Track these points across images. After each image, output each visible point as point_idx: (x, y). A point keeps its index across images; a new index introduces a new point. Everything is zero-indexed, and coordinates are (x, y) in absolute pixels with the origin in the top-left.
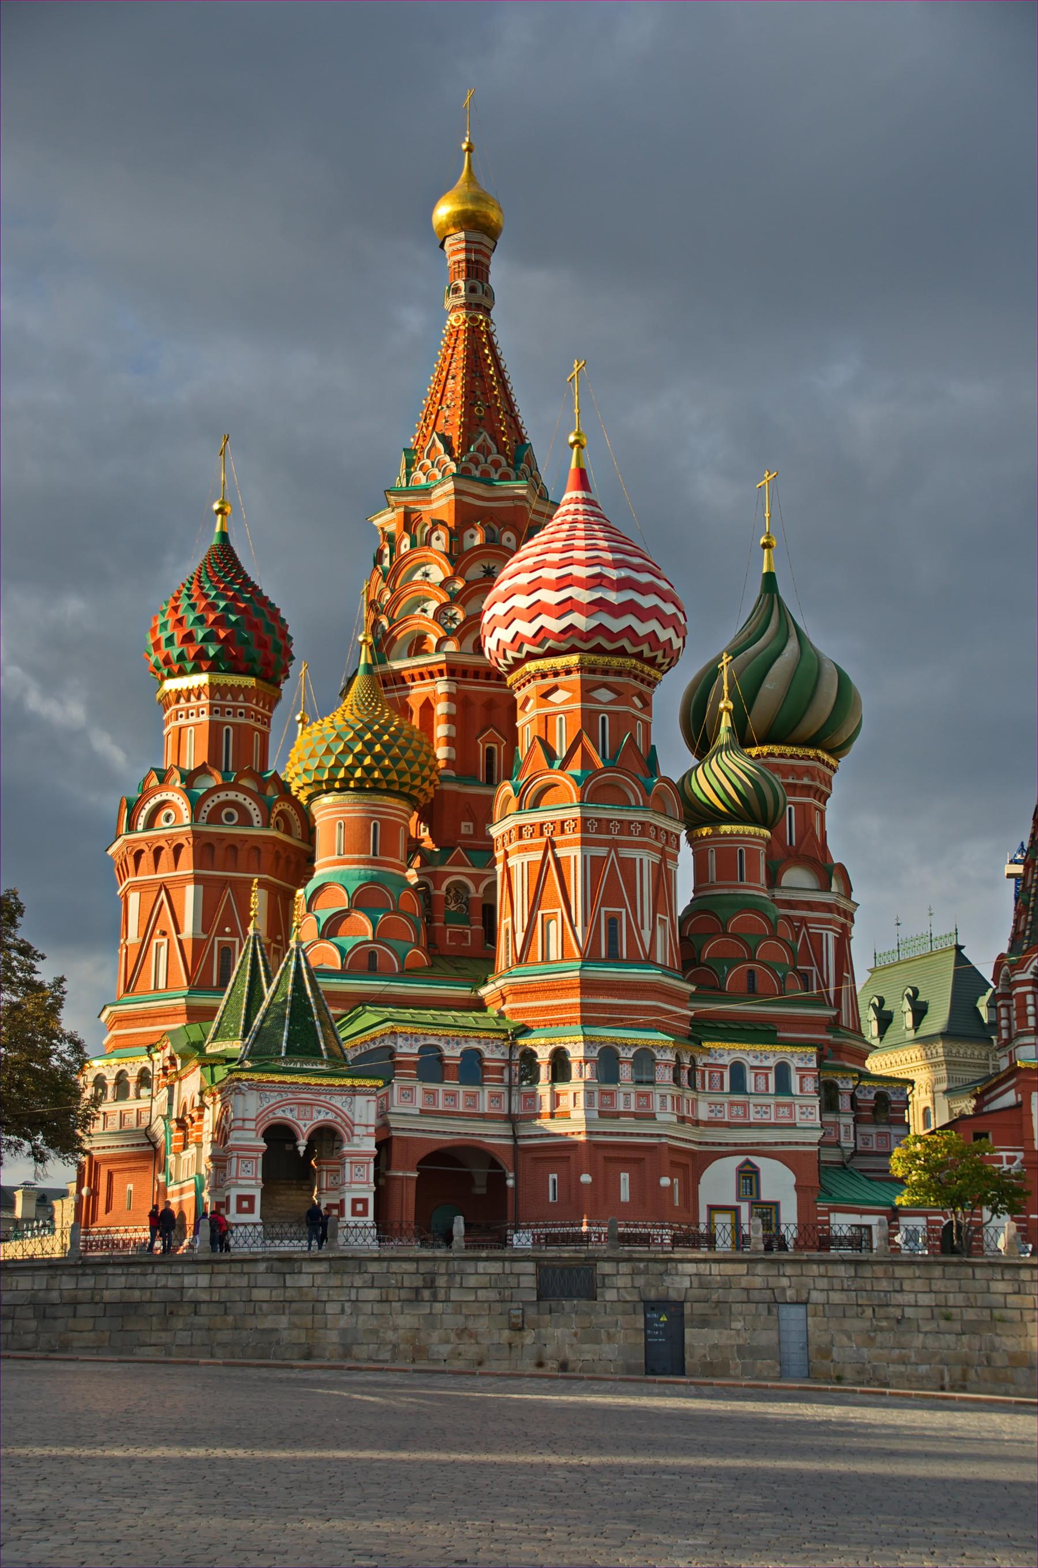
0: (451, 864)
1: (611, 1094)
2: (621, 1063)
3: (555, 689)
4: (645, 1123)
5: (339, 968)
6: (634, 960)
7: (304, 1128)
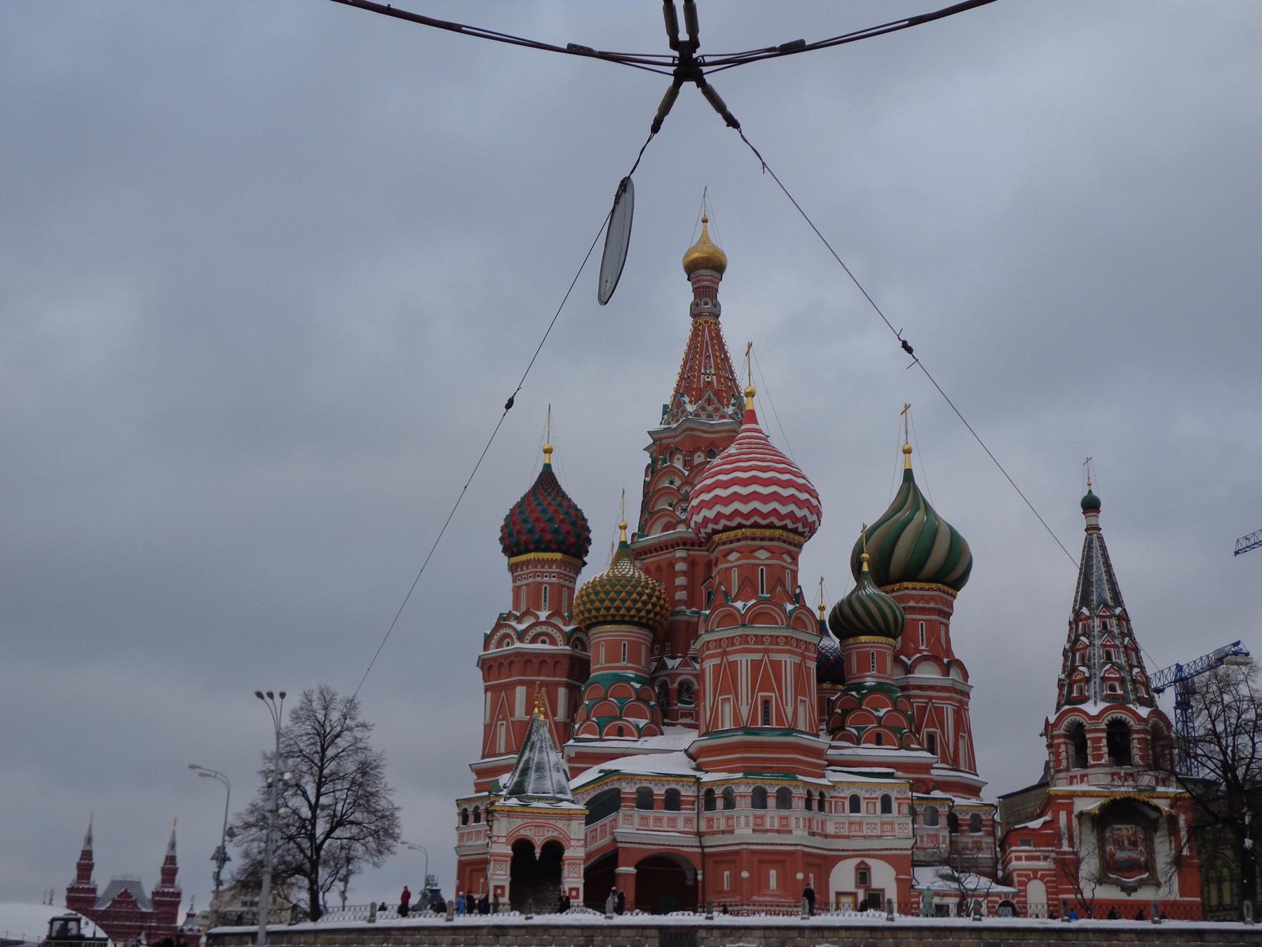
1: (762, 818)
2: (769, 796)
3: (731, 551)
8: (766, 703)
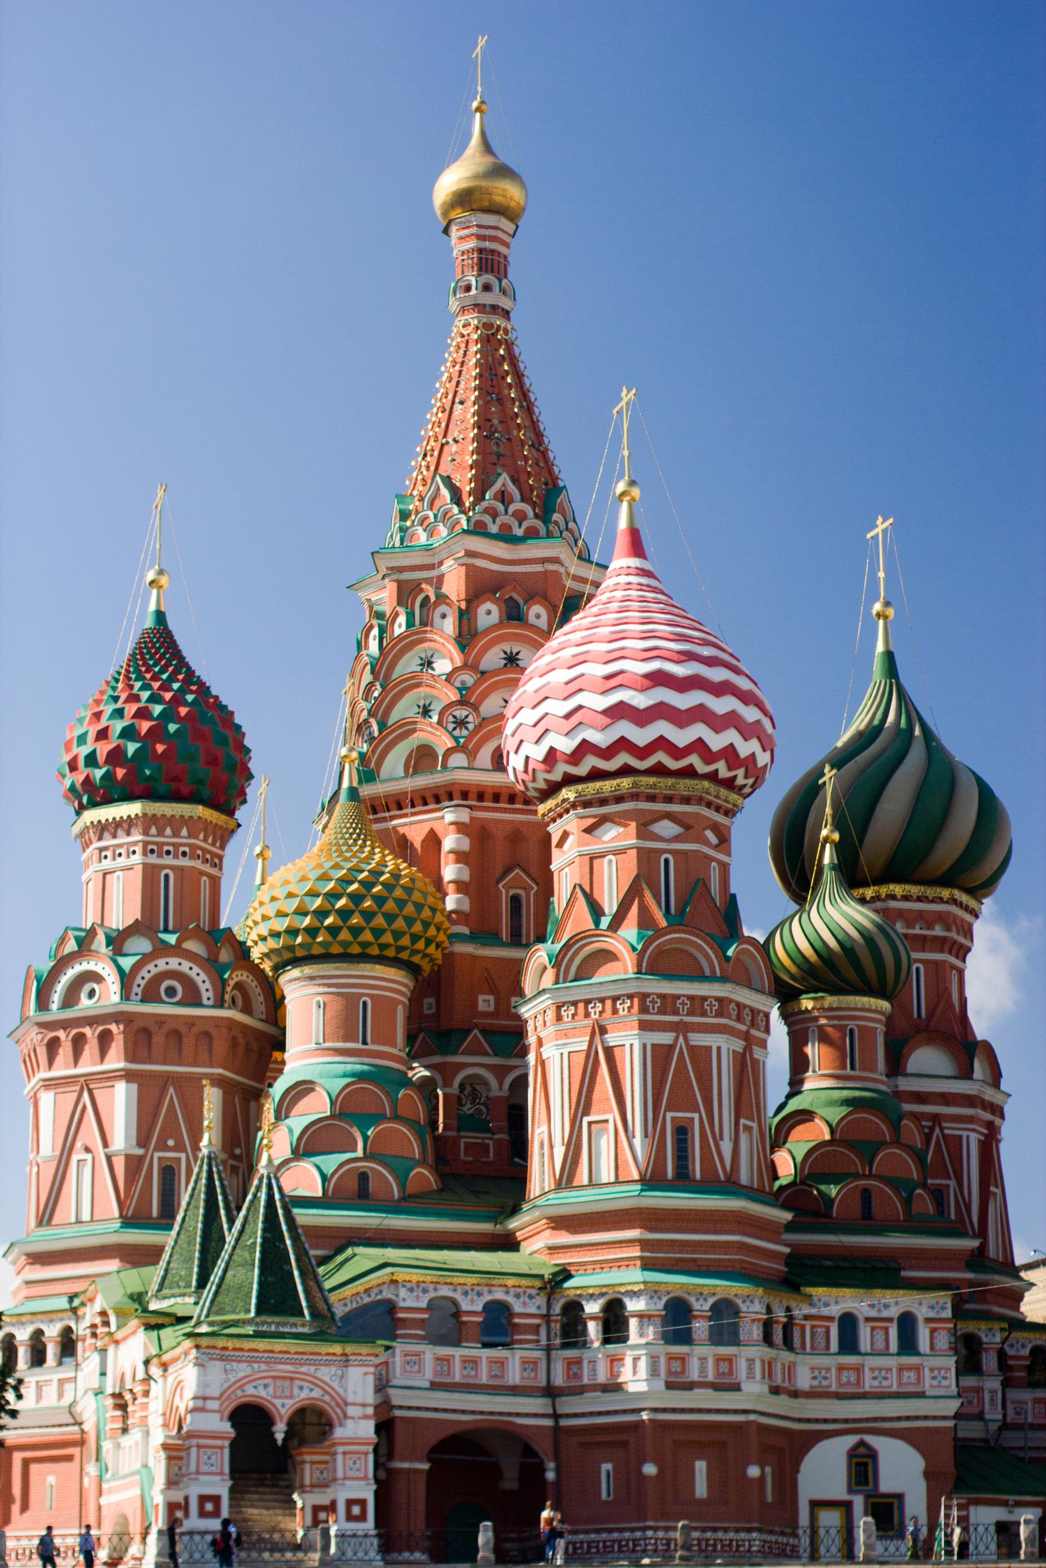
0: (465, 1053)
1: (682, 1359)
2: (695, 1317)
5: (320, 1194)
6: (710, 1185)
7: (283, 1408)
8: (682, 1132)
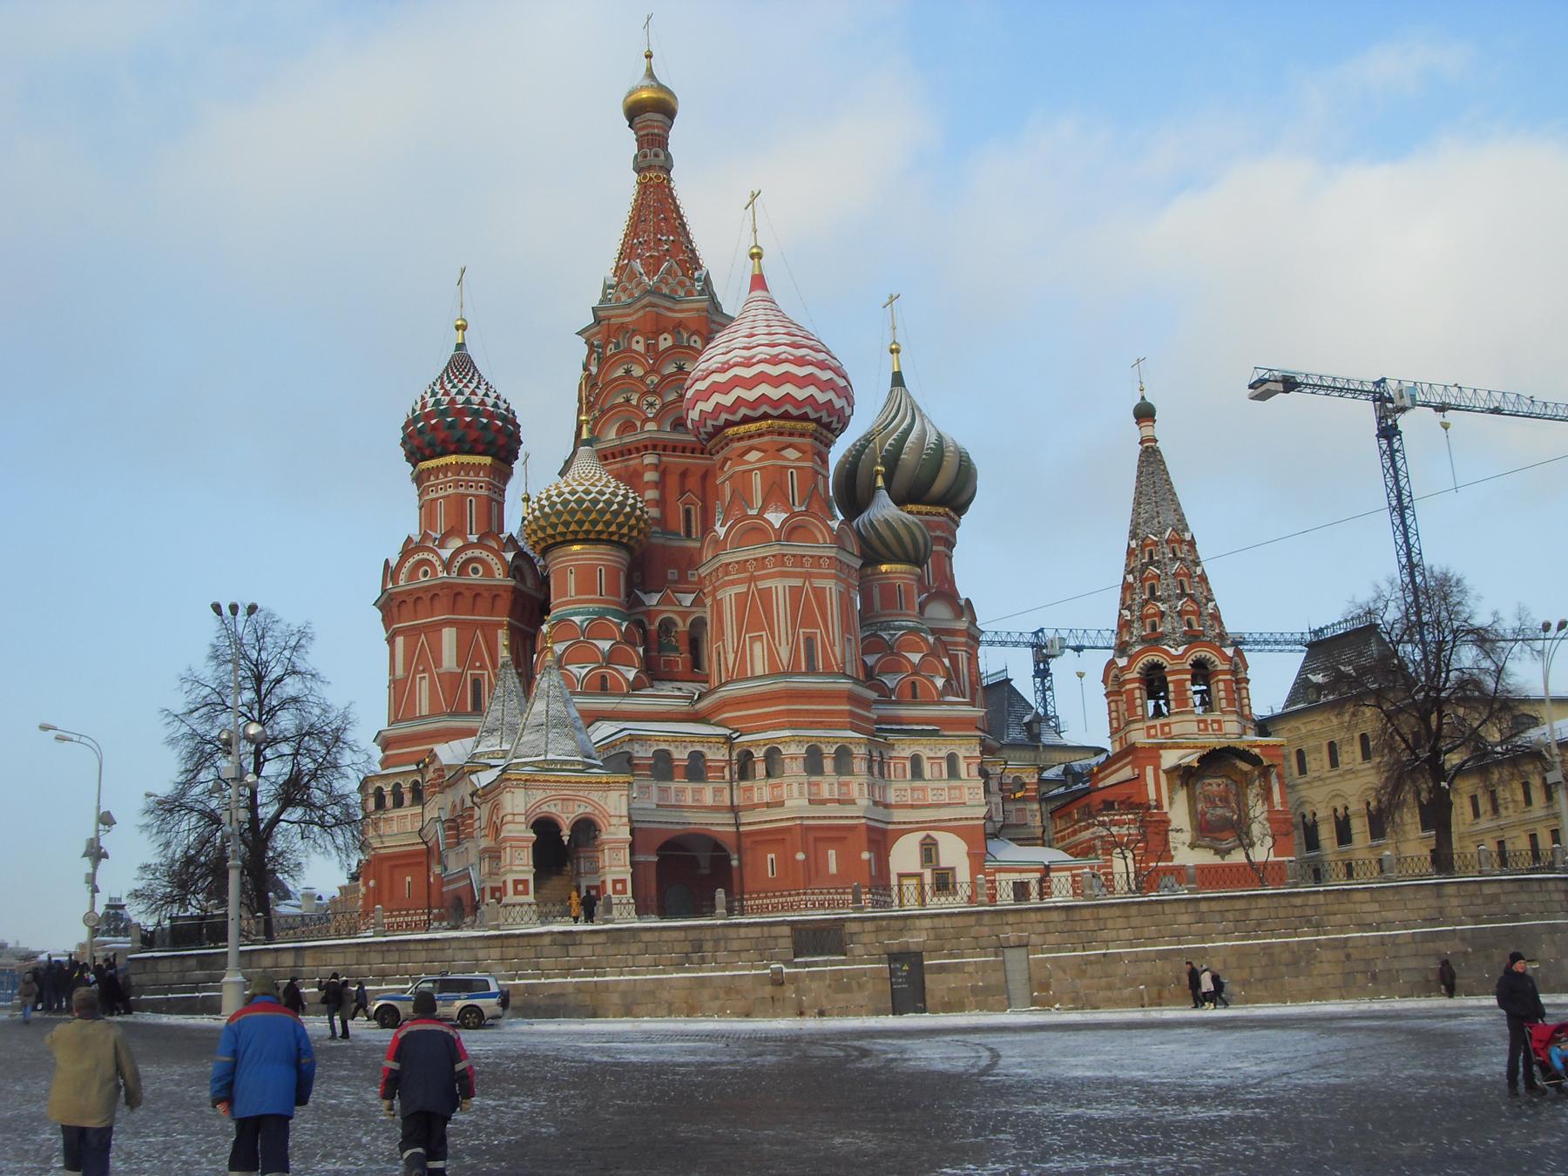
4: (848, 807)
6: (829, 673)
